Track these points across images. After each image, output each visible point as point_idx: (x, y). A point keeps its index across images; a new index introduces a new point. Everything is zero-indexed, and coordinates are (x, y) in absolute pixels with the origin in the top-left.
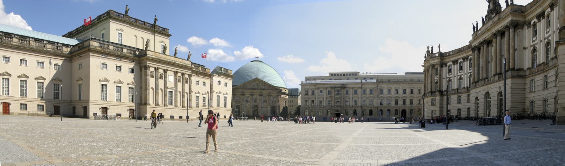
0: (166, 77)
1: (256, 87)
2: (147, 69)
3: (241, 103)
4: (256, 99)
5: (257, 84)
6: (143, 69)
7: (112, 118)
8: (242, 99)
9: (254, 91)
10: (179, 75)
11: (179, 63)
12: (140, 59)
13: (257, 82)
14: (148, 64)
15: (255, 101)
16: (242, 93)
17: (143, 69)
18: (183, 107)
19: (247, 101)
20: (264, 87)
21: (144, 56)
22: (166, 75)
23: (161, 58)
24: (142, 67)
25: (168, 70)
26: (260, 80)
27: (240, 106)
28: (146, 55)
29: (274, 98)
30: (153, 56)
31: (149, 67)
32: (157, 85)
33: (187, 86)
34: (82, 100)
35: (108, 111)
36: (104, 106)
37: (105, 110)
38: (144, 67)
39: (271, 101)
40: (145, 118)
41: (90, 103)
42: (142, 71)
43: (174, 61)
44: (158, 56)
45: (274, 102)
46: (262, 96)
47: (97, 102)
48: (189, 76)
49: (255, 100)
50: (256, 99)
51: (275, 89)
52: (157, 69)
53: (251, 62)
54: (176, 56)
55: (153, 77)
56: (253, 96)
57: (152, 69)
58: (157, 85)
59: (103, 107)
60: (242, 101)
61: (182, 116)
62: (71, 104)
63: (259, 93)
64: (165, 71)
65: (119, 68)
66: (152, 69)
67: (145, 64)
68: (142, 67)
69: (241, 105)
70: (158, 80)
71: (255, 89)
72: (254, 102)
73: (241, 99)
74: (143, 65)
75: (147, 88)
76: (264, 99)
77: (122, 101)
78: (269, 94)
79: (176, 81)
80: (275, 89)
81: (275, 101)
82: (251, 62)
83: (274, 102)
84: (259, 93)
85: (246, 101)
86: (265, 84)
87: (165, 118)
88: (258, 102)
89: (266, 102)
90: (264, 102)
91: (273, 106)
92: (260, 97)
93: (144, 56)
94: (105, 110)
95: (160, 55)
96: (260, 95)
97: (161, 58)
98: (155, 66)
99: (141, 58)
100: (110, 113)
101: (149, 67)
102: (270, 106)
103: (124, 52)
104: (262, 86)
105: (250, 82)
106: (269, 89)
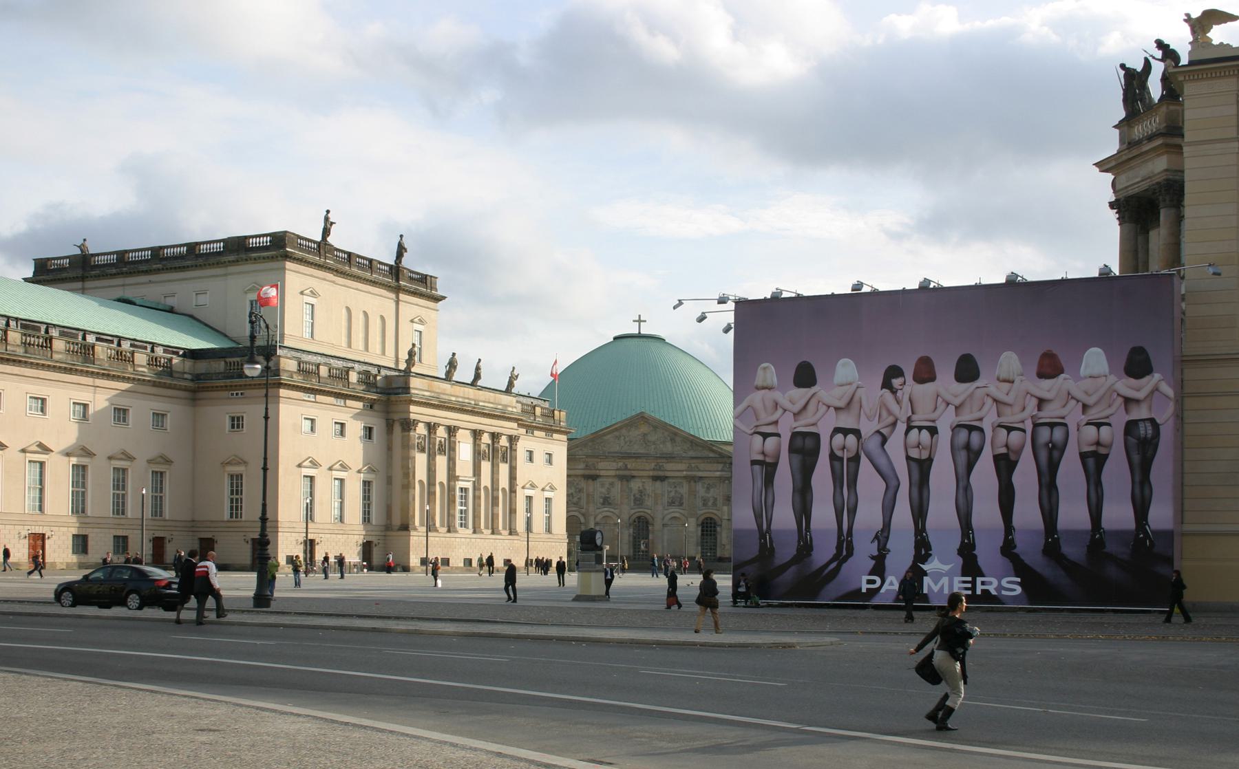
0: (454, 450)
1: (637, 449)
2: (409, 430)
3: (583, 511)
4: (641, 492)
5: (645, 435)
6: (397, 429)
8: (588, 495)
9: (631, 464)
11: (486, 404)
12: (388, 399)
13: (644, 429)
14: (412, 416)
15: (639, 501)
16: (587, 472)
17: (397, 429)
19: (606, 501)
20: (668, 448)
21: (402, 393)
22: (455, 442)
23: (444, 394)
24: (394, 421)
25: (459, 428)
26: (655, 419)
27: (582, 520)
28: (406, 389)
29: (712, 490)
31: (416, 422)
33: (504, 469)
34: (243, 519)
38: (402, 424)
39: (699, 503)
40: (406, 569)
41: (280, 530)
43: (475, 401)
44: (434, 390)
45: (710, 504)
46: (666, 482)
47: (294, 525)
49: (637, 496)
50: (641, 492)
51: (712, 455)
54: (480, 383)
55: (423, 450)
56: (628, 481)
57: (421, 430)
60: (588, 503)
63: (654, 470)
64: (452, 431)
66: (421, 430)
67: (403, 416)
68: (394, 421)
69: (583, 515)
70: (434, 459)
71: (637, 457)
72: (632, 504)
73: (584, 496)
74: (396, 417)
75: (409, 482)
76: (672, 494)
77: (346, 520)
78: (689, 473)
80: (712, 455)
81: (716, 499)
83: (710, 504)
84: (654, 470)
85: (601, 500)
86: (674, 434)
87: (450, 565)
88: (649, 502)
89: (681, 504)
90: (672, 503)
91: (707, 519)
92: (658, 484)
93: (400, 391)
95: (439, 388)
96: (656, 478)
97: (444, 394)
99: (393, 398)
101: (416, 422)
102: (697, 519)
103: (350, 380)
104: (664, 443)
105: (616, 430)
106: (691, 454)
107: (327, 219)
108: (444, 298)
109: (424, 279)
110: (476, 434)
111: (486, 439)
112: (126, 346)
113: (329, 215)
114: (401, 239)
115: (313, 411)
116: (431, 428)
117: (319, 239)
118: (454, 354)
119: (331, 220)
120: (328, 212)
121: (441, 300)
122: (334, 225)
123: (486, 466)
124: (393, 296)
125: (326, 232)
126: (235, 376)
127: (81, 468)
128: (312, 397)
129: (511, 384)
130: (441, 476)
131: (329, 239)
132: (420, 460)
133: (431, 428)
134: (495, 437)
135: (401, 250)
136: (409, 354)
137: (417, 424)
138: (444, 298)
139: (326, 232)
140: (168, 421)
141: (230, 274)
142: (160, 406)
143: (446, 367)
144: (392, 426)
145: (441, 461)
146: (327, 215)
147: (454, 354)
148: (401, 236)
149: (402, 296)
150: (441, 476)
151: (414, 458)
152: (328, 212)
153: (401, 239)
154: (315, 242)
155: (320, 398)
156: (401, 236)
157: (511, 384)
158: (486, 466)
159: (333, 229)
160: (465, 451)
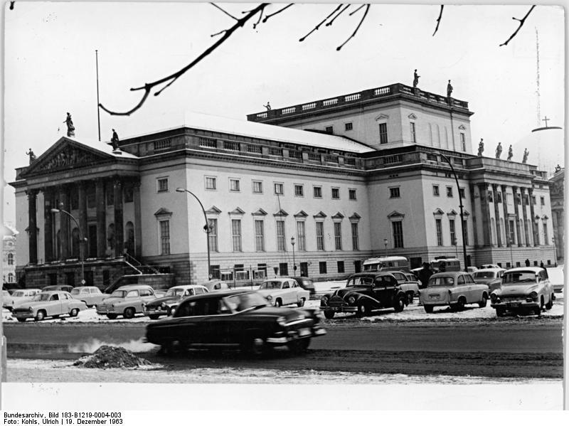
10: (519, 191)
18: (528, 245)
31: (487, 185)
36: (261, 262)
48: (530, 190)
53: (533, 131)
55: (491, 201)
57: (490, 188)
64: (504, 187)
66: (490, 188)
67: (481, 181)
79: (517, 201)
82: (533, 131)
101: (487, 185)
107: (415, 75)
108: (473, 113)
109: (464, 104)
110: (514, 188)
111: (519, 191)
112: (316, 152)
115: (436, 181)
116: (495, 186)
117: (412, 86)
118: (500, 143)
120: (416, 70)
123: (520, 207)
124: (449, 114)
125: (416, 82)
129: (525, 158)
130: (501, 215)
131: (418, 86)
132: (491, 205)
133: (495, 186)
134: (522, 189)
135: (450, 88)
138: (473, 113)
139: (416, 82)
140: (357, 194)
141: (367, 110)
142: (352, 186)
145: (500, 205)
147: (500, 143)
149: (453, 114)
150: (501, 215)
152: (416, 70)
155: (439, 174)
157: (525, 158)
158: (520, 207)
159: (419, 79)
160: (510, 200)
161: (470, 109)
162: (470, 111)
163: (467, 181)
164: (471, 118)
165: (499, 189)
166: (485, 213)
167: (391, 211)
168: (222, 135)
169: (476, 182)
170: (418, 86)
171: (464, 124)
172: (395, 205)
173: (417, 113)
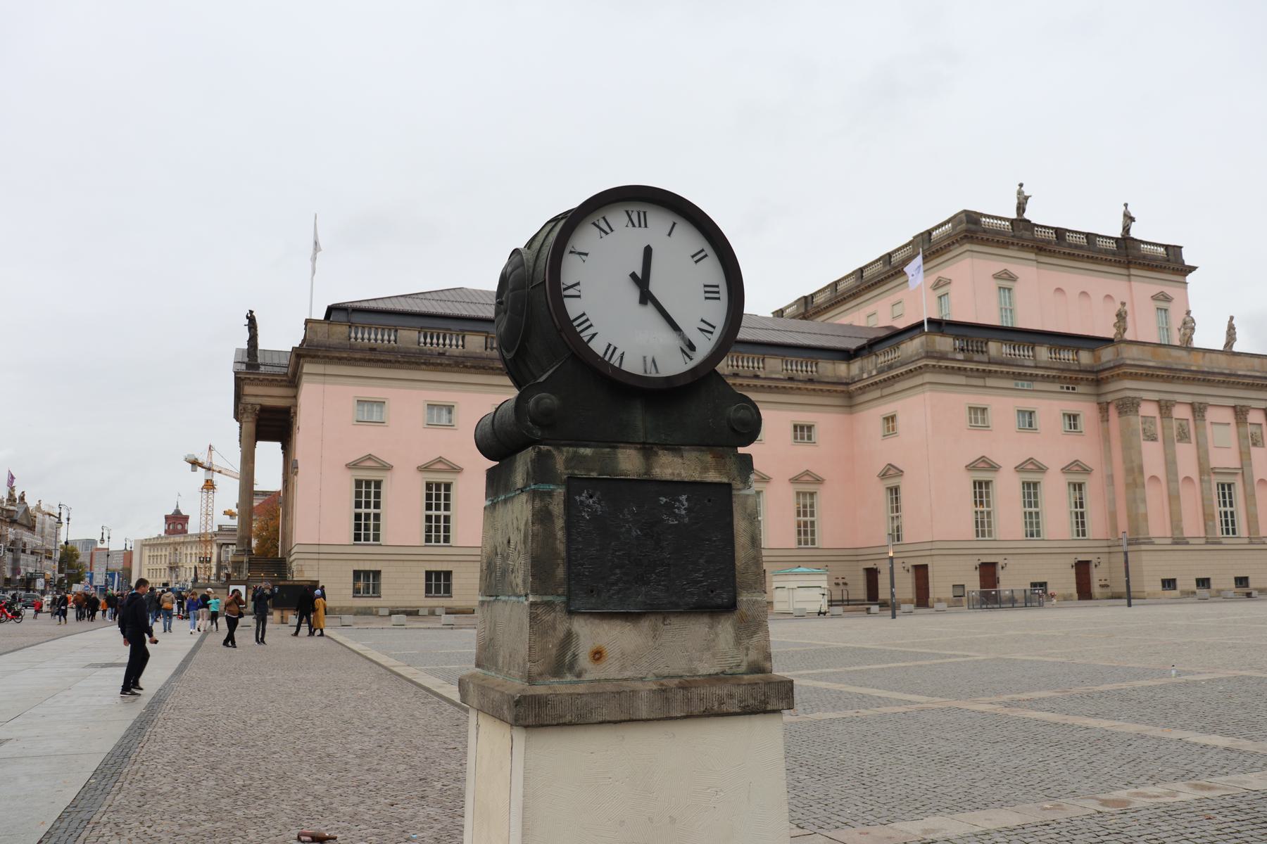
6: (1113, 412)
7: (1012, 602)
17: (1113, 412)
30: (1145, 360)
32: (1170, 464)
35: (1001, 574)
37: (988, 572)
42: (1108, 420)
52: (1165, 408)
57: (1148, 410)
58: (1170, 464)
59: (985, 561)
61: (1174, 580)
62: (1107, 550)
65: (1027, 418)
66: (1148, 410)
94: (988, 572)
98: (1156, 397)
100: (1009, 583)
107: (1020, 193)
113: (1022, 188)
114: (1126, 208)
117: (1014, 215)
119: (1026, 194)
120: (1021, 185)
121: (1190, 272)
122: (1030, 199)
125: (1021, 208)
126: (886, 369)
127: (808, 495)
128: (980, 382)
135: (1128, 218)
136: (1117, 315)
137: (1138, 405)
139: (1021, 208)
143: (1179, 330)
144: (1107, 410)
146: (1020, 188)
148: (1126, 205)
151: (1140, 446)
152: (1021, 185)
153: (1126, 208)
154: (1007, 220)
156: (1126, 205)
161: (1188, 260)
162: (1187, 263)
163: (1094, 398)
164: (1190, 278)
165: (1181, 412)
166: (1135, 472)
167: (880, 467)
168: (356, 318)
169: (1110, 398)
170: (1026, 216)
171: (1170, 290)
172: (886, 452)
173: (1014, 268)
